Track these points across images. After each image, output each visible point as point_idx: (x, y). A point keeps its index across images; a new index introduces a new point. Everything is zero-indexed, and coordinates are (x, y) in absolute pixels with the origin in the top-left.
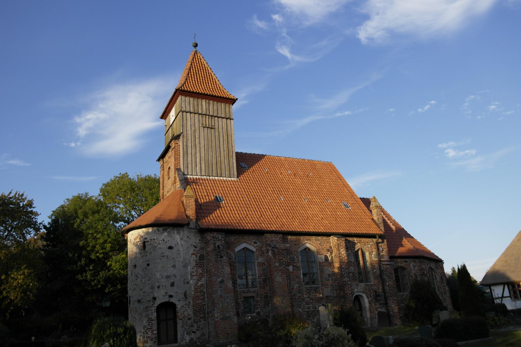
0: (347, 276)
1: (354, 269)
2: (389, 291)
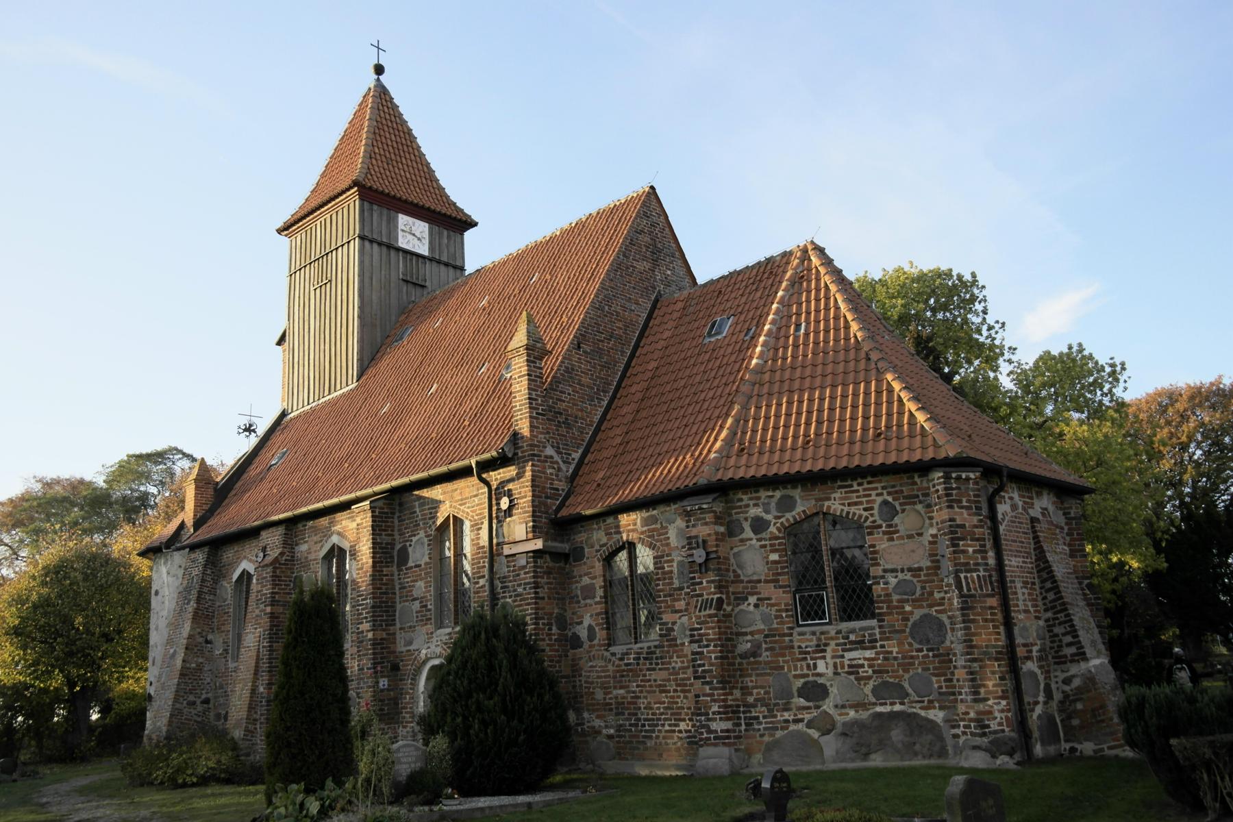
0: (366, 618)
1: (426, 587)
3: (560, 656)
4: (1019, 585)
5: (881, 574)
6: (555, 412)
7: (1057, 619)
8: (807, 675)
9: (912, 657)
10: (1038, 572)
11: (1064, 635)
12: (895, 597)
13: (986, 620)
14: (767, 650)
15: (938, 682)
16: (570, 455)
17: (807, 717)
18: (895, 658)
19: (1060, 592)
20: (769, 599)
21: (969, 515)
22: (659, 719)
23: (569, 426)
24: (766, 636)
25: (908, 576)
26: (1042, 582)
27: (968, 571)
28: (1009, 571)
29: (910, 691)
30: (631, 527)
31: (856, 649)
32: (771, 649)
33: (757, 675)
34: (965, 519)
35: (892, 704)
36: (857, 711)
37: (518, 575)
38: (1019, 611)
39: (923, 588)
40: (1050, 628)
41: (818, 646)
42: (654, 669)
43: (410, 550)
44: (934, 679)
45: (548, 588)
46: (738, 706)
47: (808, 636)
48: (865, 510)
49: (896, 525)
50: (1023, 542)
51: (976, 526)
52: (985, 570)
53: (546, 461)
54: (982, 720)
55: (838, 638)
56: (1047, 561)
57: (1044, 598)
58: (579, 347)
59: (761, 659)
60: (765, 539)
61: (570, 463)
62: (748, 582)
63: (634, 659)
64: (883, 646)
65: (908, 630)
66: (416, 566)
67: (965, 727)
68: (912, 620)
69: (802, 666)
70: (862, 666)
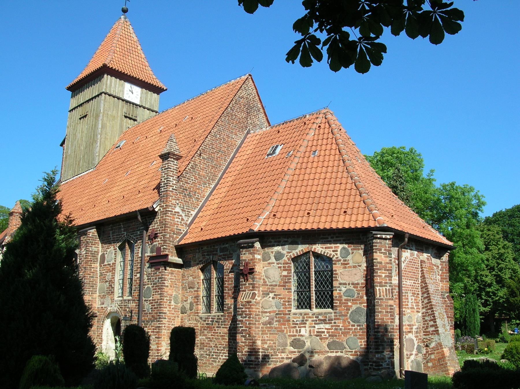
2: (150, 312)
4: (410, 294)
5: (338, 285)
6: (183, 189)
7: (428, 312)
8: (296, 336)
9: (349, 329)
10: (421, 288)
11: (430, 321)
12: (344, 298)
13: (387, 312)
14: (276, 321)
15: (361, 342)
16: (190, 212)
18: (341, 329)
19: (430, 299)
20: (279, 295)
21: (385, 257)
22: (221, 353)
23: (190, 197)
24: (277, 314)
25: (351, 287)
26: (423, 294)
27: (380, 286)
28: (405, 287)
29: (346, 346)
30: (215, 253)
31: (322, 323)
32: (279, 321)
33: (270, 334)
34: (382, 259)
35: (336, 352)
36: (318, 355)
37: (156, 273)
38: (408, 308)
39: (358, 294)
40: (424, 317)
41: (303, 321)
42: (220, 327)
43: (106, 256)
44: (359, 340)
45: (171, 281)
47: (297, 316)
48: (333, 251)
49: (348, 260)
50: (415, 273)
51: (388, 263)
52: (390, 286)
53: (175, 215)
54: (379, 362)
55: (313, 317)
56: (426, 283)
57: (423, 302)
59: (273, 326)
60: (281, 264)
61: (189, 217)
62: (270, 285)
63: (211, 321)
64: (335, 323)
65: (349, 315)
66: (109, 264)
67: (371, 365)
68: (351, 310)
69: (293, 331)
70: (324, 332)
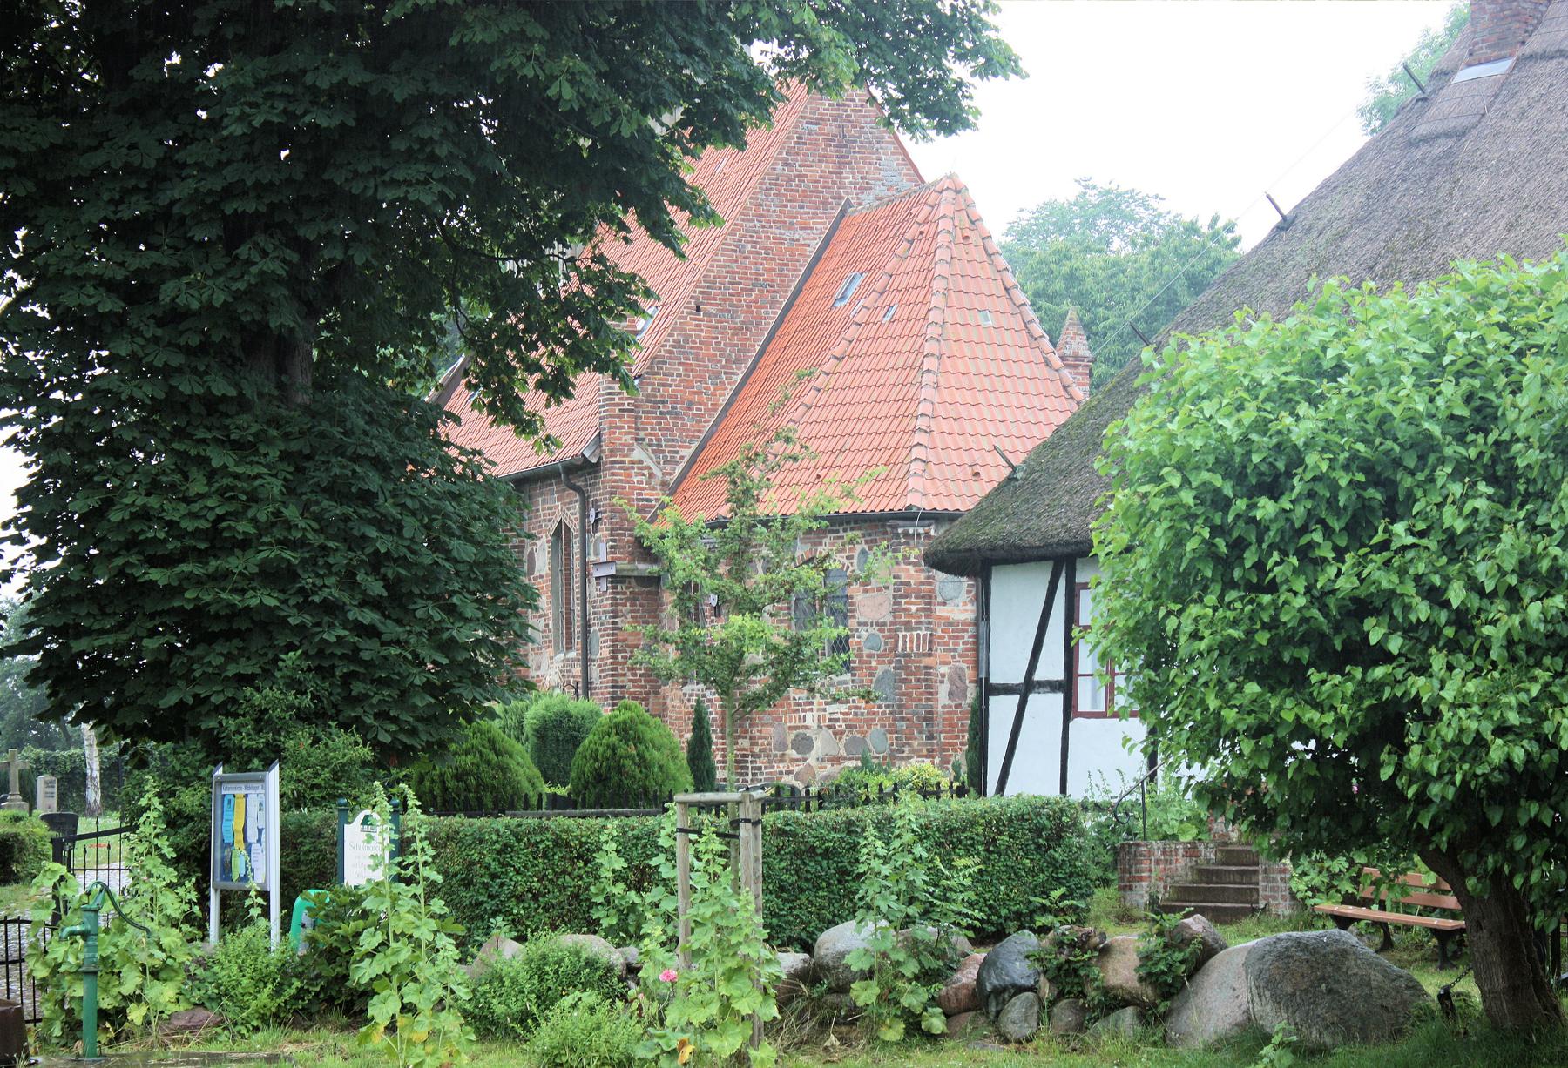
3: (648, 693)
12: (866, 652)
17: (796, 769)
23: (677, 416)
25: (874, 630)
46: (745, 756)
58: (698, 309)
